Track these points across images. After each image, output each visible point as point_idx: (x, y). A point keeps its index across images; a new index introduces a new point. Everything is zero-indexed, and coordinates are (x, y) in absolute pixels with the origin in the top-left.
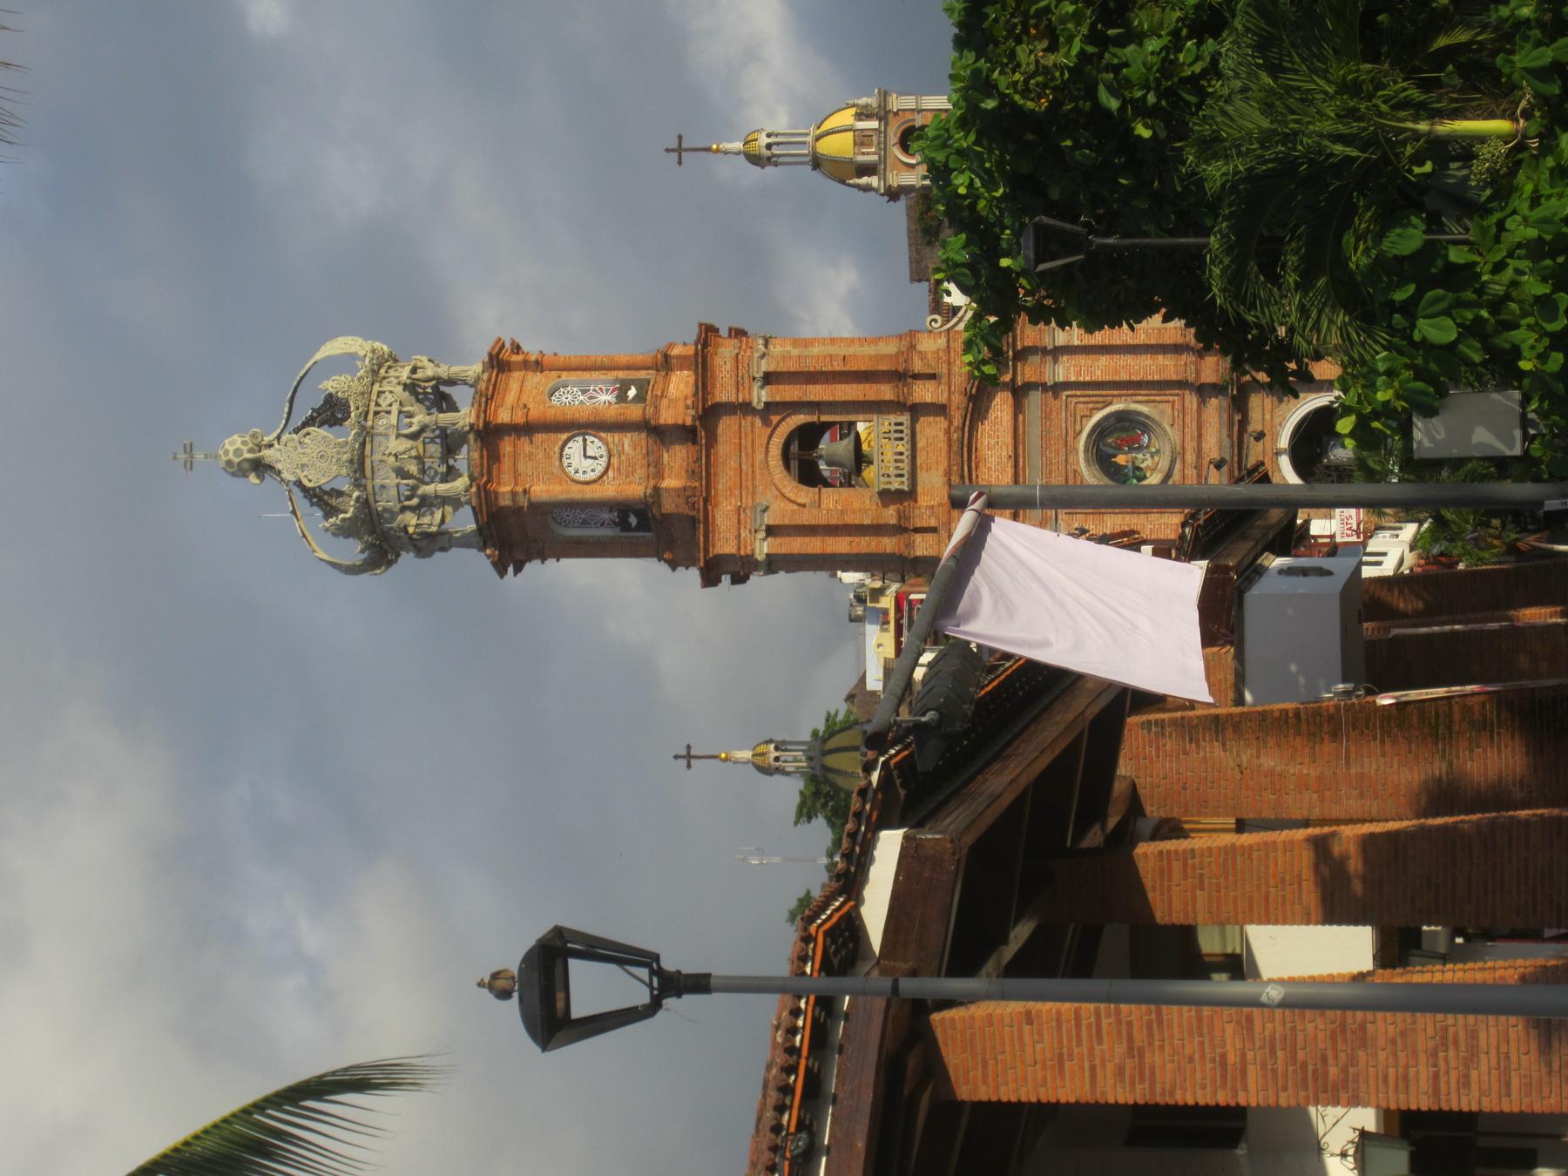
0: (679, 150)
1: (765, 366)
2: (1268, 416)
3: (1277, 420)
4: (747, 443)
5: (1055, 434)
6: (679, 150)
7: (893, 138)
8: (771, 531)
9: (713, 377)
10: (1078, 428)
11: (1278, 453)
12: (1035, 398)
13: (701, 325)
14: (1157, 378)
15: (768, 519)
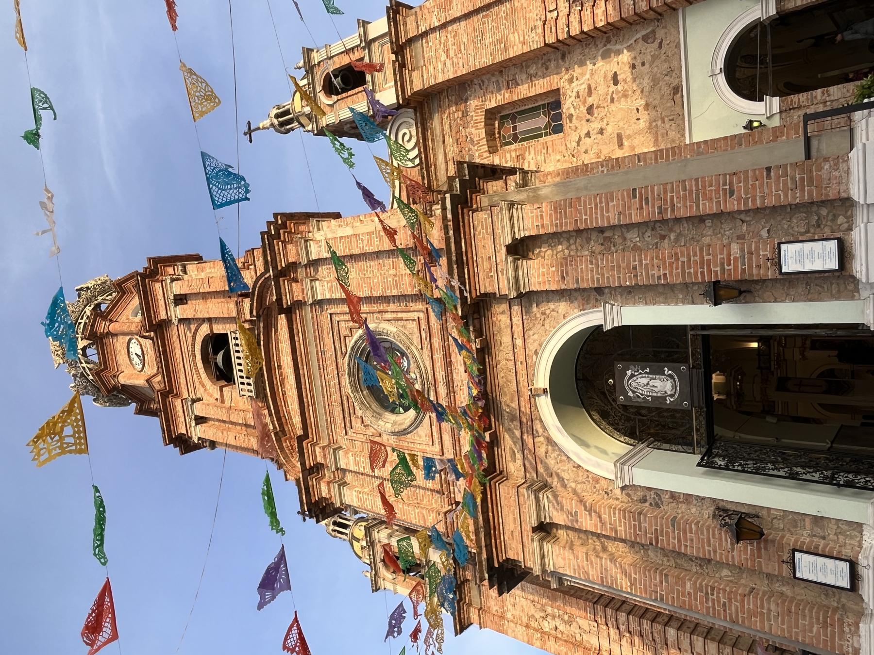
0: (249, 132)
1: (178, 288)
2: (519, 342)
3: (532, 347)
4: (185, 350)
5: (328, 355)
6: (249, 132)
7: (319, 88)
8: (200, 420)
9: (155, 300)
10: (343, 348)
11: (534, 394)
12: (308, 313)
13: (149, 259)
14: (394, 292)
15: (199, 410)
